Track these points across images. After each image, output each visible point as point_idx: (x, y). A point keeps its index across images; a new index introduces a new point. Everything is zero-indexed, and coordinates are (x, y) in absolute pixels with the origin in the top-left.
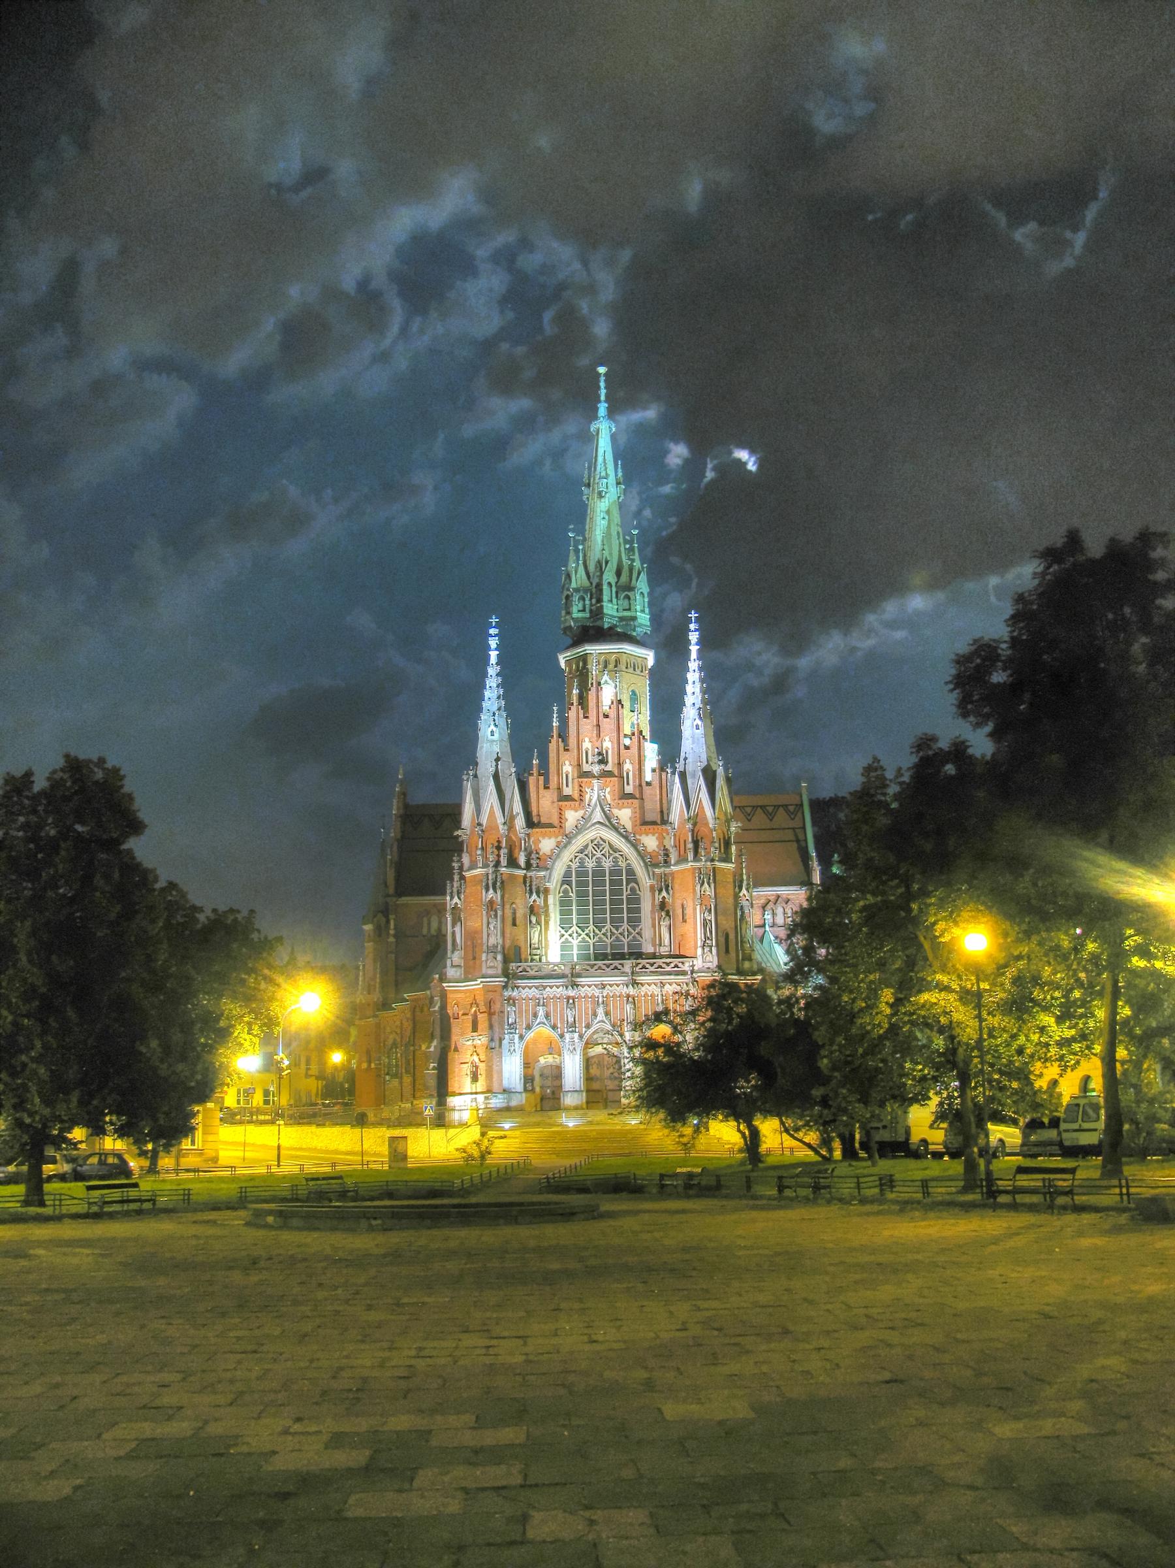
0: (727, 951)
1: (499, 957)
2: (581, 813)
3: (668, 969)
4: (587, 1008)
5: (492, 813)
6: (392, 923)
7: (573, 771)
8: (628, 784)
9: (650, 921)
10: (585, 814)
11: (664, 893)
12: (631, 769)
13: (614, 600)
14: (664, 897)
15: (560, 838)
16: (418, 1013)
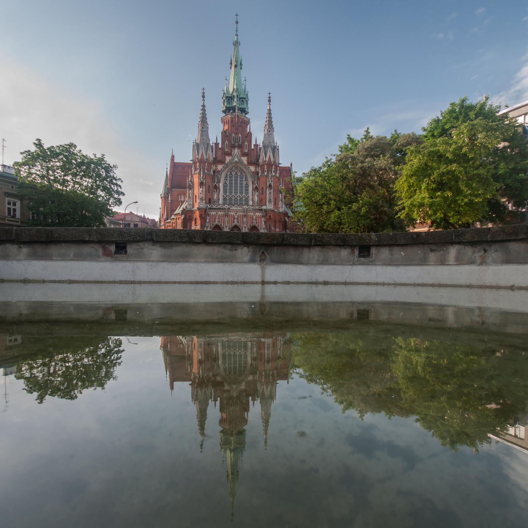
0: (275, 205)
1: (204, 201)
2: (231, 157)
3: (257, 208)
4: (231, 219)
5: (202, 155)
6: (170, 196)
7: (229, 143)
8: (246, 149)
9: (251, 193)
10: (232, 158)
11: (256, 185)
12: (247, 144)
13: (239, 101)
14: (256, 186)
15: (224, 165)
16: (177, 220)
